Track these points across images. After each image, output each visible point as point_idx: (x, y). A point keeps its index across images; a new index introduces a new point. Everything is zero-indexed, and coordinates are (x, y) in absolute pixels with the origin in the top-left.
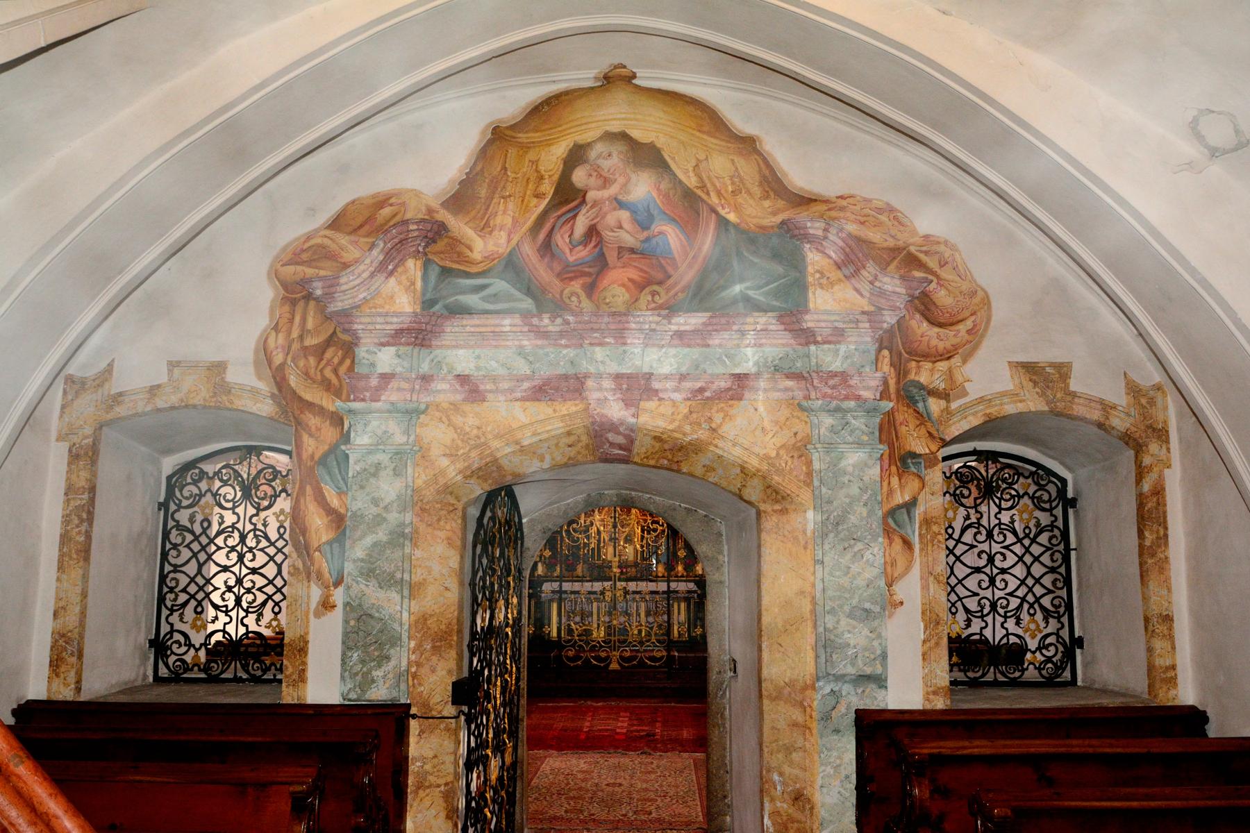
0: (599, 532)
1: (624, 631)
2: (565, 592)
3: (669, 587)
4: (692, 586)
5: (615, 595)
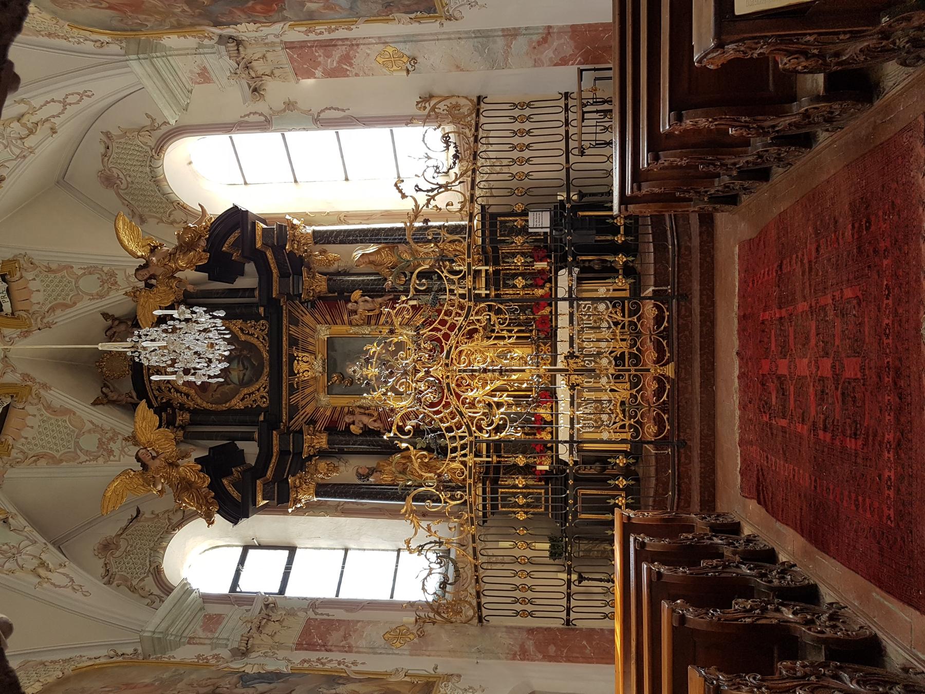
0: (492, 394)
1: (619, 360)
2: (571, 436)
3: (564, 299)
4: (563, 273)
5: (575, 370)
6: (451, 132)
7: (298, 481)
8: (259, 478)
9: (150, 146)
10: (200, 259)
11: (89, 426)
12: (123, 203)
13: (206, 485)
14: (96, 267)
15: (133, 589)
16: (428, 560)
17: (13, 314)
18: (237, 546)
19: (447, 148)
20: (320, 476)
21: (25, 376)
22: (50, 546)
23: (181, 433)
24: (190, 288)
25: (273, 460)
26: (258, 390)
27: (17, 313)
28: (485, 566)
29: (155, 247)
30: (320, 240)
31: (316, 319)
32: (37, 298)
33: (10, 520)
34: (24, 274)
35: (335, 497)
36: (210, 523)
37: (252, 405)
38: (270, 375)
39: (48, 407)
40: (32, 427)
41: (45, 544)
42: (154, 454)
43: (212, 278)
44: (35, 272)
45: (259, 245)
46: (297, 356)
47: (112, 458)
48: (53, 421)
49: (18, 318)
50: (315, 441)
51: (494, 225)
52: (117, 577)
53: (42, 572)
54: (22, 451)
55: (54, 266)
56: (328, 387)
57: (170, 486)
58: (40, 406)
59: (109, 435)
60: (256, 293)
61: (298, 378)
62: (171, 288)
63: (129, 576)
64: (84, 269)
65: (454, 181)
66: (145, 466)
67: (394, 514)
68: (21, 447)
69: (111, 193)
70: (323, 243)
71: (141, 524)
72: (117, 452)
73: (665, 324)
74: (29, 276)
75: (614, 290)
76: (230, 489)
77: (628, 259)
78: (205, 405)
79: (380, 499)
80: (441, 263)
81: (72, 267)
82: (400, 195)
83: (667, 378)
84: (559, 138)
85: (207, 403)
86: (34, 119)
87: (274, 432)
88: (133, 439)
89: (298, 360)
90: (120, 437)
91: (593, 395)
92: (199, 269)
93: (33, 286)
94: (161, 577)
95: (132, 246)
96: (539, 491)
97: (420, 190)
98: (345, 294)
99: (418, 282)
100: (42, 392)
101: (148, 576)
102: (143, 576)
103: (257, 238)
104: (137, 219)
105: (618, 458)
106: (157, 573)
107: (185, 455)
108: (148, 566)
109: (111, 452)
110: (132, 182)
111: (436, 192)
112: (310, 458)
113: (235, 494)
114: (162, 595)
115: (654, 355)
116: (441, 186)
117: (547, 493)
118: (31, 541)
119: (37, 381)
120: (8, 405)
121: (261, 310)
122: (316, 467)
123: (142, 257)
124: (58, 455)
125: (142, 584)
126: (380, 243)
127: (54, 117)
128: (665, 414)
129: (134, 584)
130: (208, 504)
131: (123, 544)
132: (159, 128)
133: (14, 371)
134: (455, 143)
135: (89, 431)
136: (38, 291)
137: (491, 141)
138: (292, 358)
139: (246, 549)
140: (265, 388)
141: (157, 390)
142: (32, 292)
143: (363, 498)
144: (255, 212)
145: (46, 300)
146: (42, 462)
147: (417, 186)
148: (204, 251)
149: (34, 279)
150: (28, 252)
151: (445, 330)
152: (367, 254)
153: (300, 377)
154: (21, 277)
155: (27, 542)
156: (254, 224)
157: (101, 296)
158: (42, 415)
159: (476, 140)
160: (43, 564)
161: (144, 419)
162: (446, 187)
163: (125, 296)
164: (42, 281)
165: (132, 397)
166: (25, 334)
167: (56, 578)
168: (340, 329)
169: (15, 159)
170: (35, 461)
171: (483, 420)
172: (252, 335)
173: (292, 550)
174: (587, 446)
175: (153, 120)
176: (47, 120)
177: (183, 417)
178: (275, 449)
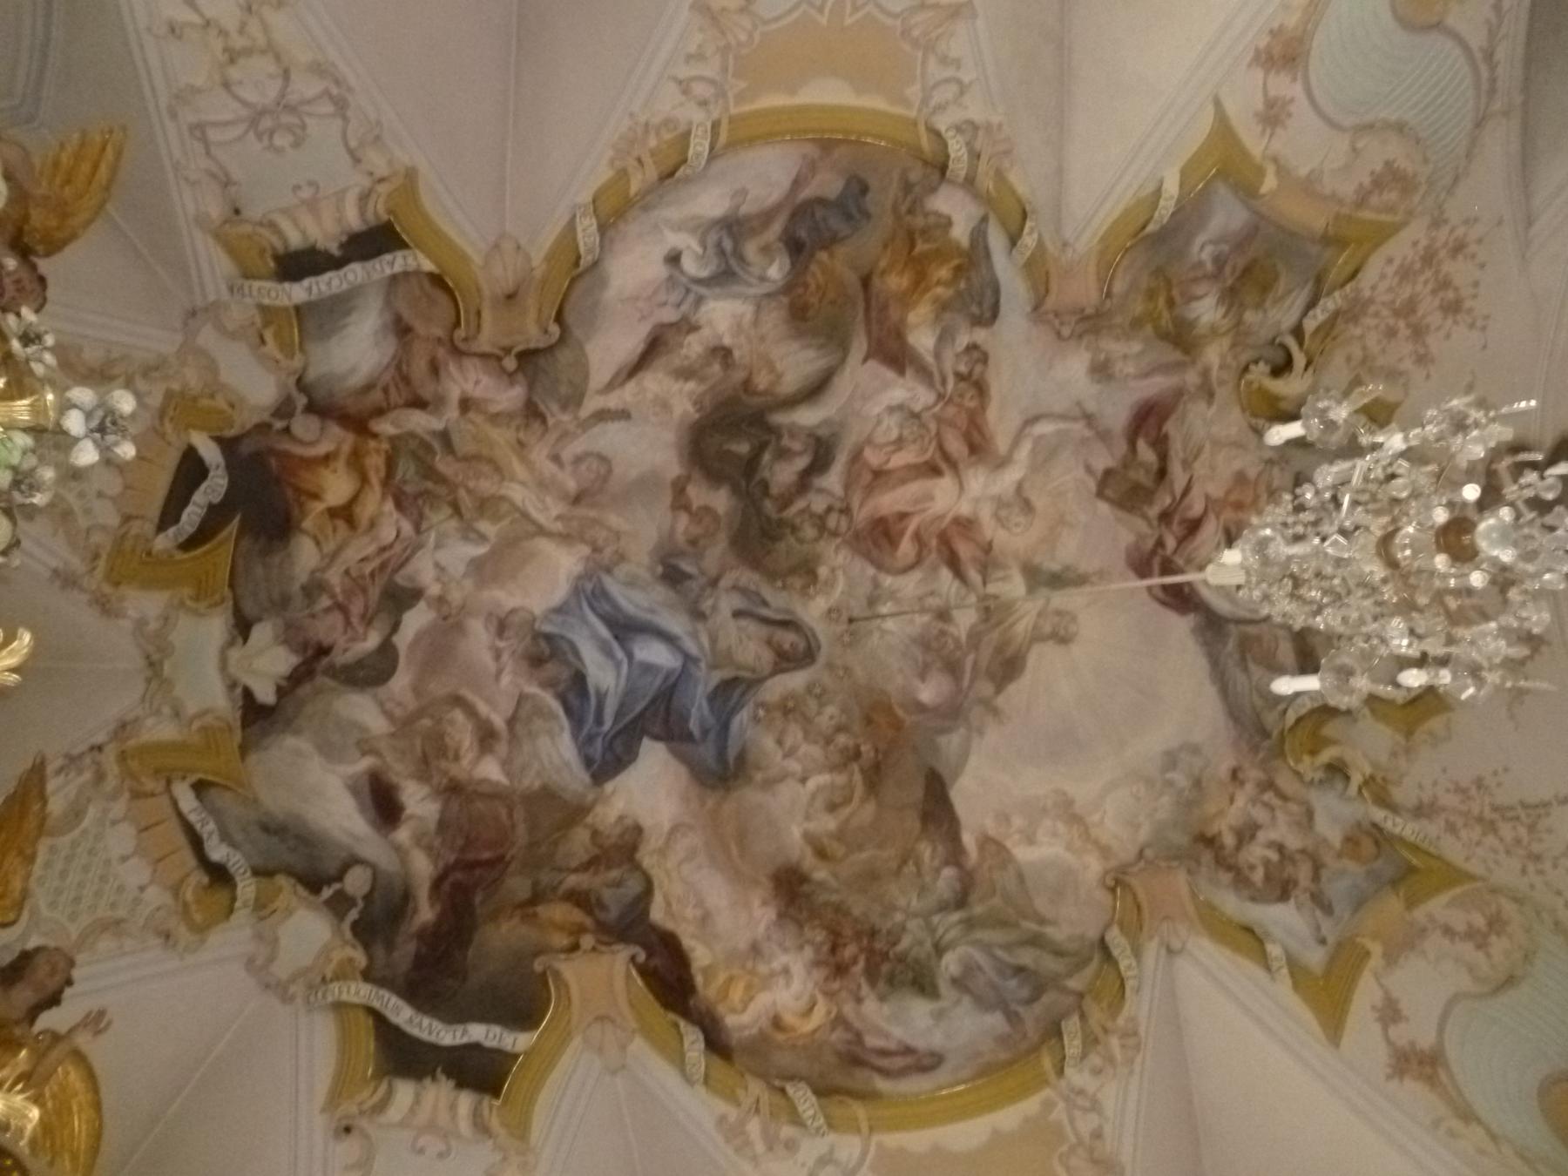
17: (169, 782)
32: (121, 839)
34: (167, 899)
41: (173, 115)
49: (157, 771)
58: (83, 522)
74: (156, 896)
93: (136, 873)
100: (77, 564)
118: (205, 141)
119: (85, 597)
136: (124, 859)
142: (139, 851)
149: (142, 889)
164: (121, 889)
166: (123, 728)
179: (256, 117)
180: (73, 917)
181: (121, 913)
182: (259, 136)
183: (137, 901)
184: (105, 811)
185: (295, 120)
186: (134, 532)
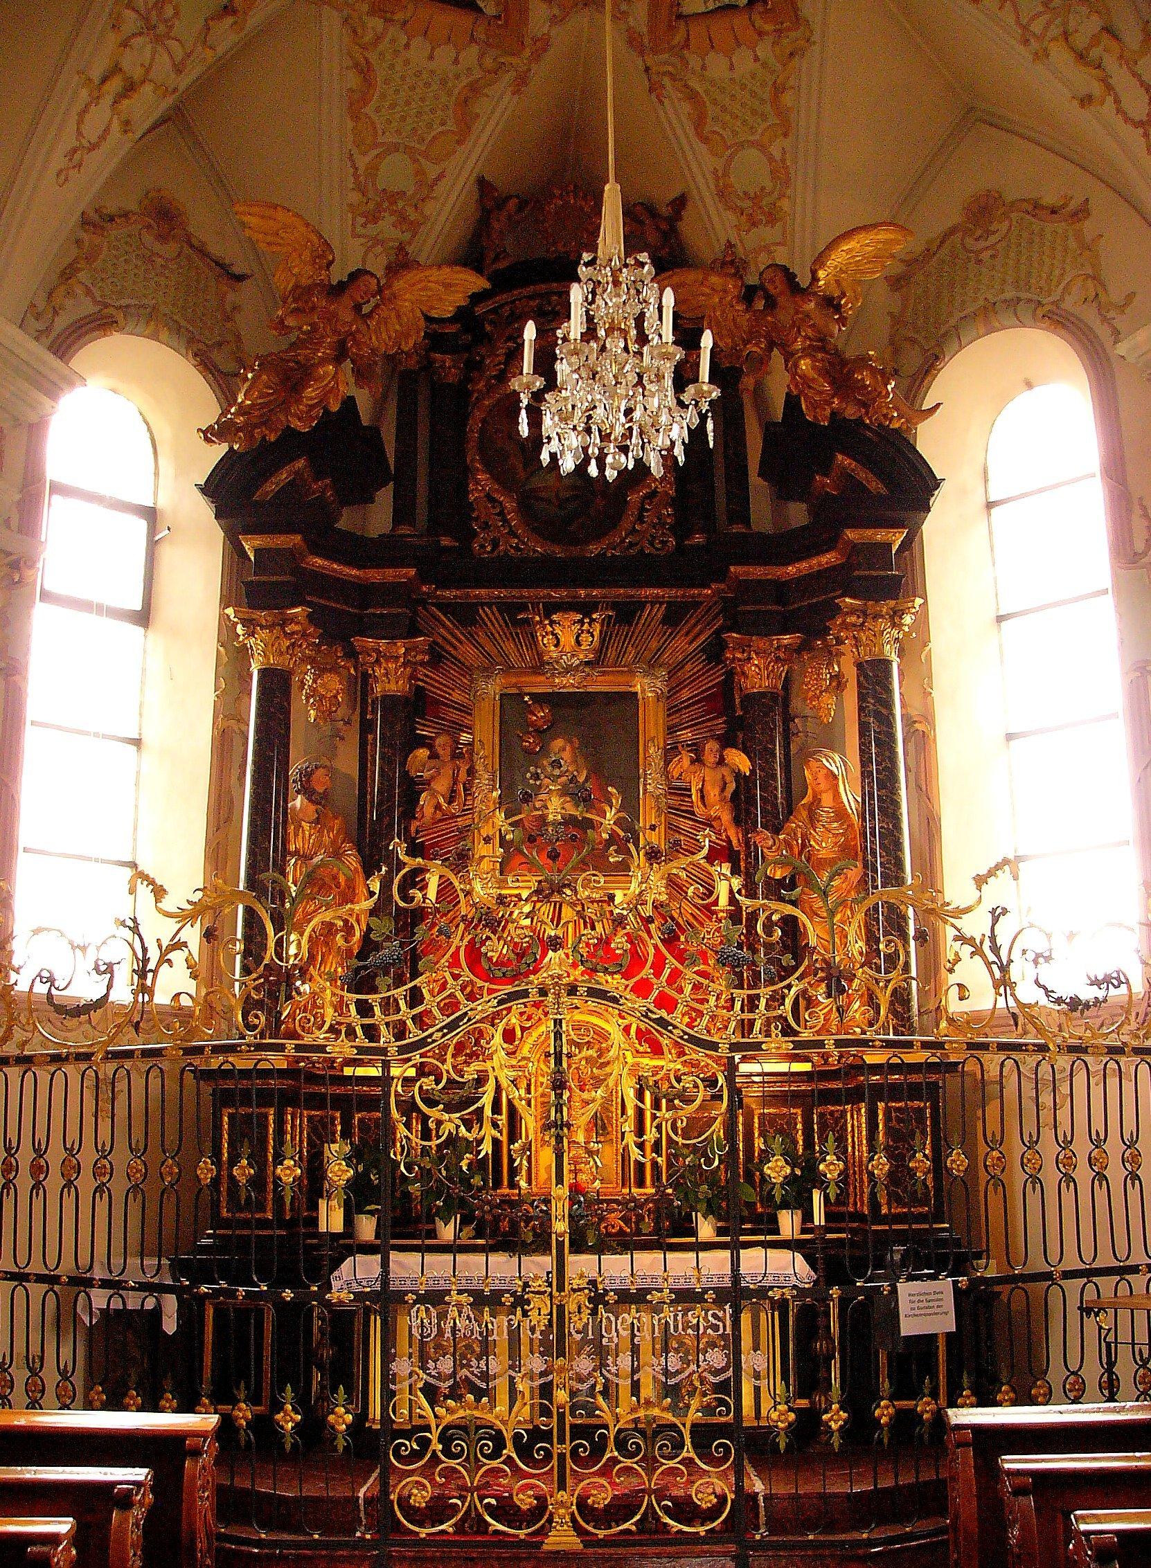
2: (400, 1296)
5: (561, 1308)
6: (1129, 989)
7: (297, 628)
8: (305, 540)
9: (1062, 299)
10: (814, 406)
11: (432, 171)
12: (929, 242)
13: (296, 424)
14: (787, 182)
15: (68, 274)
16: (104, 943)
17: (680, 16)
18: (156, 494)
19: (1096, 983)
20: (309, 678)
21: (543, 44)
22: (169, 101)
23: (413, 364)
24: (748, 382)
25: (347, 570)
26: (513, 534)
27: (682, 23)
28: (90, 1073)
29: (838, 308)
30: (866, 676)
31: (681, 665)
32: (717, 66)
33: (230, 20)
34: (769, 40)
35: (258, 715)
36: (209, 435)
37: (477, 519)
38: (546, 560)
39: (474, 89)
40: (431, 58)
41: (175, 90)
42: (366, 309)
43: (771, 432)
44: (772, 61)
45: (851, 534)
46: (592, 621)
47: (361, 220)
48: (444, 99)
50: (392, 666)
51: (914, 1091)
52: (97, 240)
53: (115, 84)
54: (378, 39)
55: (787, 99)
56: (521, 695)
57: (293, 346)
58: (477, 74)
59: (413, 216)
60: (736, 529)
61: (541, 622)
62: (746, 342)
63: (98, 264)
64: (783, 161)
65: (1016, 1000)
66: (341, 288)
67: (218, 855)
68: (389, 36)
69: (955, 217)
70: (860, 685)
71: (213, 283)
72: (372, 230)
73: (675, 1526)
74: (764, 50)
75: (757, 1390)
76: (284, 476)
77: (836, 1434)
78: (478, 414)
79: (252, 823)
80: (821, 974)
81: (785, 135)
82: (983, 872)
83: (543, 1532)
84: (1122, 1252)
85: (484, 421)
86: (1110, 64)
87: (412, 572)
88: (401, 263)
89: (581, 622)
90: (407, 236)
91: (500, 1337)
92: (792, 403)
94: (93, 330)
95: (838, 258)
96: (270, 1205)
97: (995, 920)
98: (740, 735)
99: (775, 918)
100: (508, 77)
101: (96, 302)
102: (97, 294)
103: (869, 532)
104: (900, 269)
105: (347, 1412)
106: (102, 323)
107: (362, 375)
108: (118, 304)
109: (373, 218)
110: (979, 262)
111: (992, 957)
112: (351, 654)
113: (271, 487)
114: (54, 334)
115: (602, 1498)
116: (1004, 969)
117: (264, 1224)
118: (183, 62)
119: (534, 67)
120: (479, 10)
121: (698, 539)
122: (330, 671)
123: (815, 279)
124: (369, 110)
125: (79, 290)
126: (864, 819)
127: (1117, 101)
128: (455, 1525)
129: (82, 276)
130: (248, 428)
131: (170, 249)
132: (1105, 320)
133: (554, 21)
134: (1105, 1000)
135: (420, 172)
136: (732, 67)
137: (1113, 1082)
138: (586, 609)
139: (151, 515)
140: (517, 549)
141: (512, 313)
143: (255, 782)
144: (926, 527)
145: (713, 83)
146: (353, 80)
147: (1005, 911)
148: (833, 414)
149: (756, 59)
150: (816, 48)
151: (660, 984)
152: (837, 785)
153: (544, 627)
154: (761, 34)
155: (179, 53)
156: (897, 524)
157: (723, 193)
158: (457, 77)
159: (1114, 1051)
160: (130, 88)
161: (448, 286)
162: (1003, 983)
163: (723, 241)
164: (753, 76)
165: (496, 259)
166: (633, 40)
167: (100, 115)
168: (652, 722)
169: (1018, 22)
170: (356, 65)
171: (437, 1082)
172: (640, 519)
173: (143, 617)
174: (376, 1324)
175: (1121, 309)
176: (1109, 88)
177: (448, 365)
178: (375, 576)
179: (158, 39)
180: (764, 117)
181: (770, 80)
182: (171, 27)
183: (764, 65)
184: (694, 73)
185: (154, 13)
186: (483, 37)
